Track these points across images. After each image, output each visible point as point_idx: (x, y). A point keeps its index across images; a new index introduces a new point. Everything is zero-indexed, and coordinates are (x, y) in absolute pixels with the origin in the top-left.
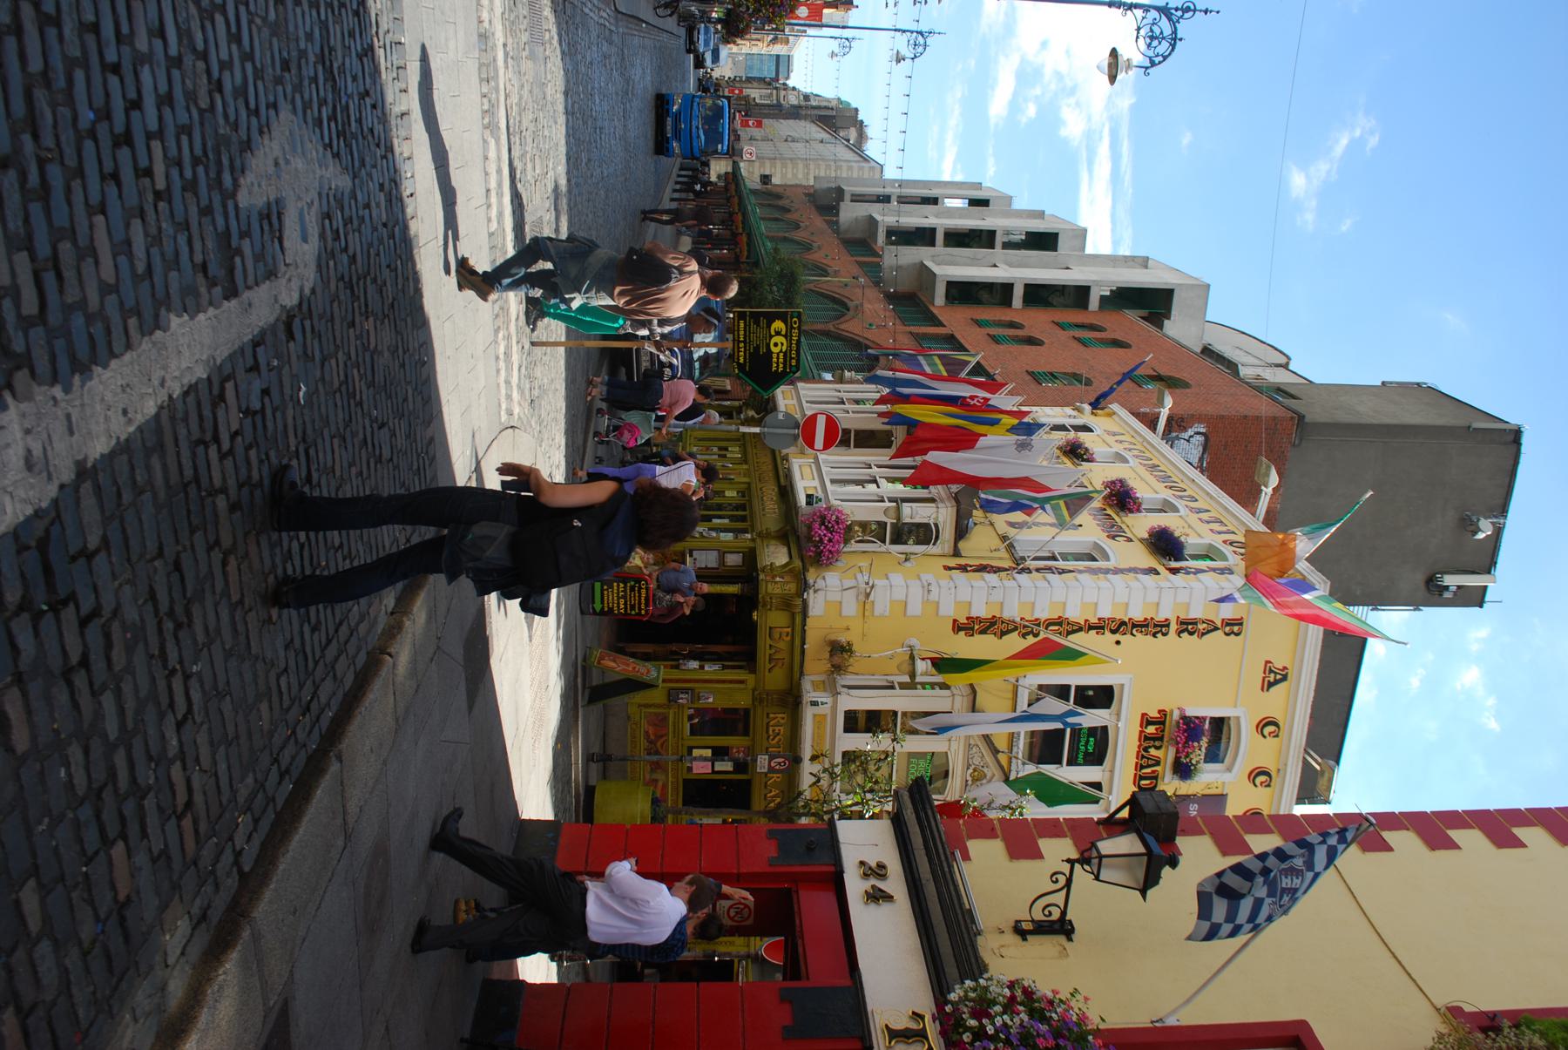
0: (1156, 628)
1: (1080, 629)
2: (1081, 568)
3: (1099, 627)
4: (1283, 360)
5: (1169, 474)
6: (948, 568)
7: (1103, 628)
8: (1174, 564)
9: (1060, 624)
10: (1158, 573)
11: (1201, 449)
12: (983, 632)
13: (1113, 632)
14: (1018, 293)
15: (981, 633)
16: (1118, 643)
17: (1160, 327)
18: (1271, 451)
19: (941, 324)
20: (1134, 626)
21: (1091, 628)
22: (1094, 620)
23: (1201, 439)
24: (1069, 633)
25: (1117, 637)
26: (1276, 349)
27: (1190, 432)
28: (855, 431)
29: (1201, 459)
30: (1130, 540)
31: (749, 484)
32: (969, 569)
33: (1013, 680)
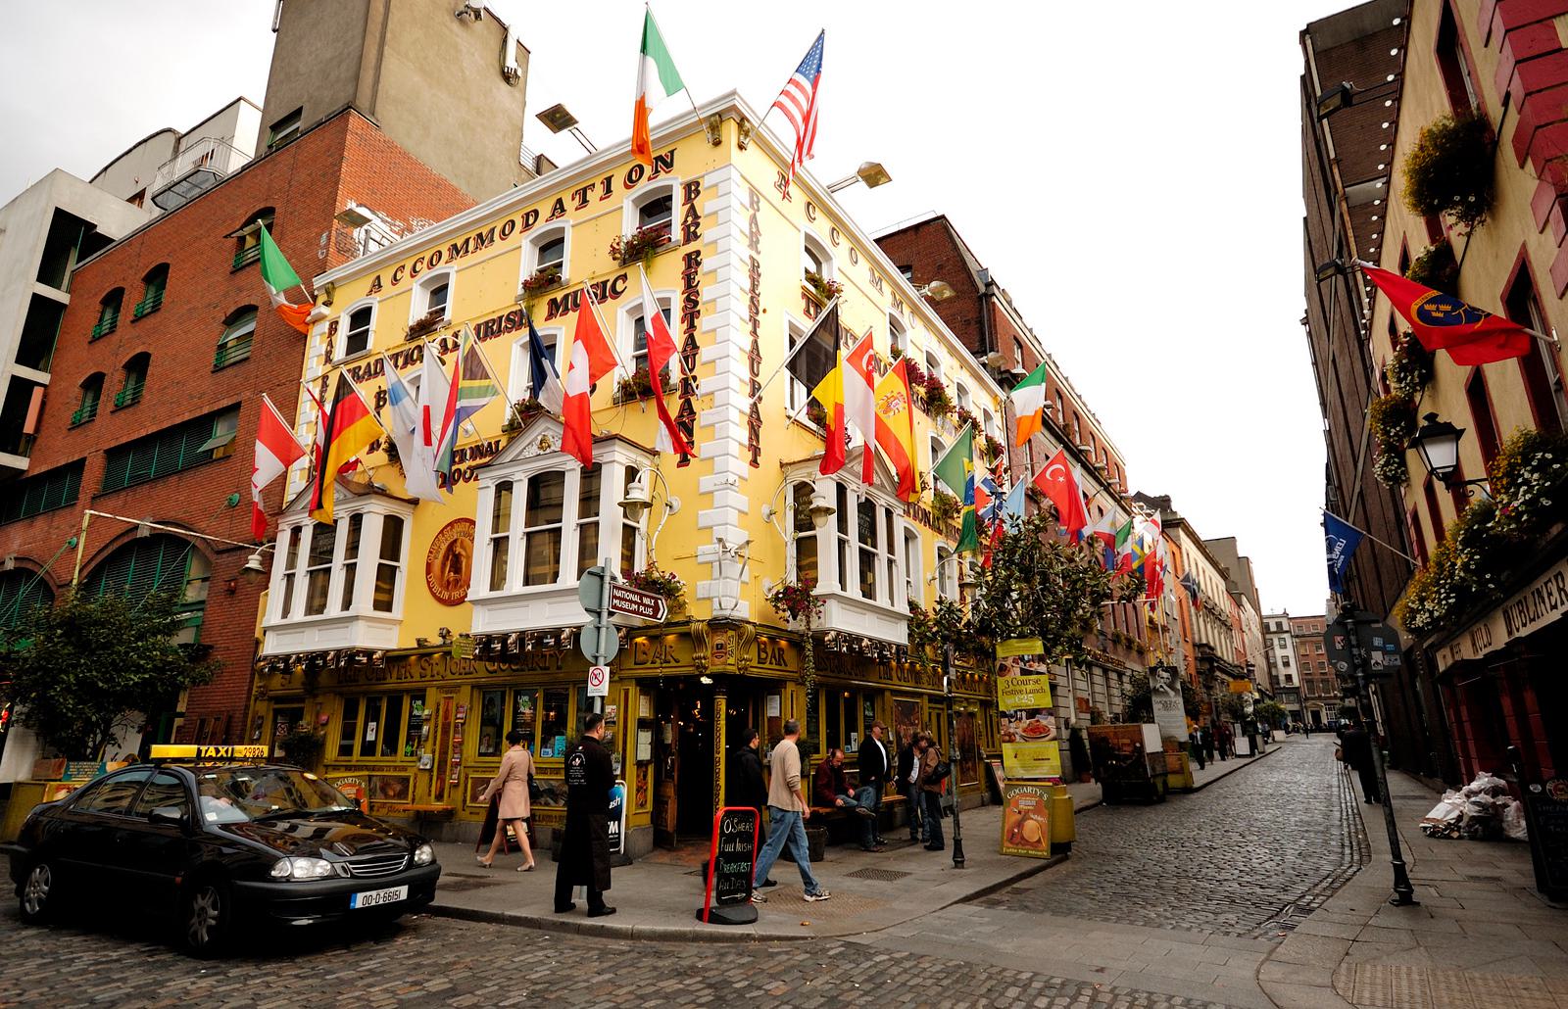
0: (755, 267)
1: (756, 342)
3: (755, 324)
4: (171, 139)
5: (473, 235)
7: (755, 320)
9: (753, 360)
10: (698, 253)
12: (757, 437)
13: (757, 313)
14: (26, 372)
15: (758, 441)
16: (764, 311)
17: (106, 240)
19: (77, 467)
20: (753, 291)
21: (754, 332)
22: (750, 327)
24: (758, 355)
25: (761, 309)
26: (145, 141)
28: (381, 557)
30: (624, 277)
31: (473, 687)
33: (788, 422)
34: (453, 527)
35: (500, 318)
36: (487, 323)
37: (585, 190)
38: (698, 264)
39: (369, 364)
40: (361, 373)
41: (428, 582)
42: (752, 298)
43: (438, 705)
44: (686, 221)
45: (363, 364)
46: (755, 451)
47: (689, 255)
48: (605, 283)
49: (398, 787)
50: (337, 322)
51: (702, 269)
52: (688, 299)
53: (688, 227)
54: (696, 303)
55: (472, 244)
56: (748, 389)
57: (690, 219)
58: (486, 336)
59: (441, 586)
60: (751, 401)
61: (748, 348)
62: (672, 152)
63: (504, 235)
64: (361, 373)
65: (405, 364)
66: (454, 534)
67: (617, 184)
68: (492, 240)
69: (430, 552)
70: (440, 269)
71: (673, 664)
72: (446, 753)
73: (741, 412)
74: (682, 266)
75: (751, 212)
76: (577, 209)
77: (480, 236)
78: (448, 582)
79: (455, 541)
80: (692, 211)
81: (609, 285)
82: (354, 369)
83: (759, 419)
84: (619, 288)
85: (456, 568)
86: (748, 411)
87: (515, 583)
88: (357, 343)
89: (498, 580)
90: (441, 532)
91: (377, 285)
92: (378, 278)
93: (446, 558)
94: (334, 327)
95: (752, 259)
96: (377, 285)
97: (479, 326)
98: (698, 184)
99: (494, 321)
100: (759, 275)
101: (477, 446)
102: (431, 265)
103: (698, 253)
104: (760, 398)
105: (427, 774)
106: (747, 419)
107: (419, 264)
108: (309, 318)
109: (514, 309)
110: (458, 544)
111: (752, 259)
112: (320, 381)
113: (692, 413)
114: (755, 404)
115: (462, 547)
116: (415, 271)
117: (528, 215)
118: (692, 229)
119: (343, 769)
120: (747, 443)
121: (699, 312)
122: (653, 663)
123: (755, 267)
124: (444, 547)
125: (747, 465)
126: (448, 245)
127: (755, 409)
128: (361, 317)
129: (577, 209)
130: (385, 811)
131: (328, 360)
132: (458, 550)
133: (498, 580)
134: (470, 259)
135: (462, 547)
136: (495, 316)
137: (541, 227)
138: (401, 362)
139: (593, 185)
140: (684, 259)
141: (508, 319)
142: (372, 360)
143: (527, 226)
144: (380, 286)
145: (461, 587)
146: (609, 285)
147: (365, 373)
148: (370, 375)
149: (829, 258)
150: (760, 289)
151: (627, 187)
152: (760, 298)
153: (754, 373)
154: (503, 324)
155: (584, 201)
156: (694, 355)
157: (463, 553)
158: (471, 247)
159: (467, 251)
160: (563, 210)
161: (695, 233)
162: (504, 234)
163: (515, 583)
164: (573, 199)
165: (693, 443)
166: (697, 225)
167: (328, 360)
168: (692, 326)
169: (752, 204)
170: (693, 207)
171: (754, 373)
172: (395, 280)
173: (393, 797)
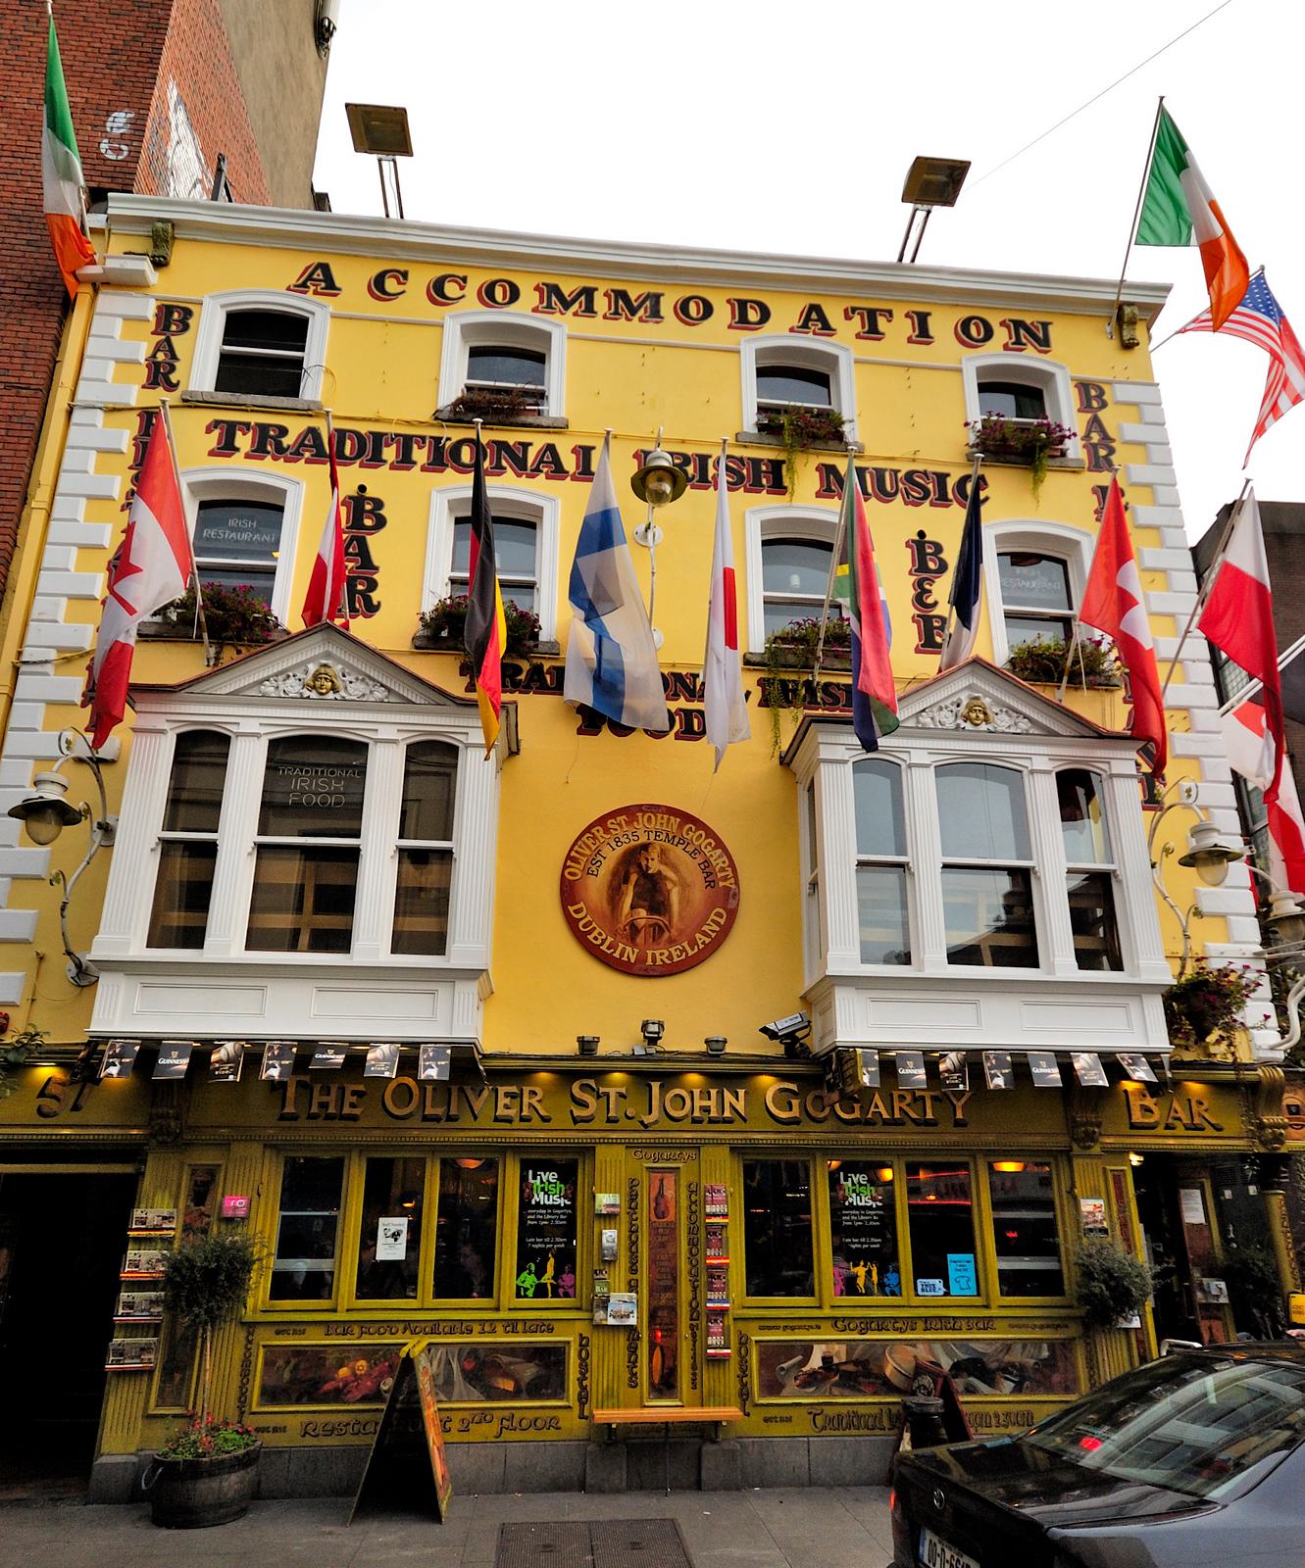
40: (287, 441)
41: (572, 923)
43: (633, 1184)
45: (296, 427)
49: (529, 1371)
50: (188, 313)
57: (1095, 438)
59: (614, 935)
62: (1045, 325)
67: (943, 324)
69: (569, 857)
71: (1209, 1131)
72: (672, 1288)
78: (634, 930)
79: (645, 847)
80: (1096, 423)
82: (263, 428)
90: (602, 821)
93: (619, 877)
94: (173, 318)
101: (678, 677)
105: (622, 1341)
110: (654, 853)
112: (134, 422)
118: (1103, 452)
119: (322, 1330)
122: (1167, 1127)
124: (611, 856)
130: (494, 1427)
132: (654, 866)
134: (596, 326)
137: (781, 332)
138: (420, 455)
145: (671, 942)
146: (951, 483)
157: (670, 874)
166: (1112, 451)
173: (516, 1394)
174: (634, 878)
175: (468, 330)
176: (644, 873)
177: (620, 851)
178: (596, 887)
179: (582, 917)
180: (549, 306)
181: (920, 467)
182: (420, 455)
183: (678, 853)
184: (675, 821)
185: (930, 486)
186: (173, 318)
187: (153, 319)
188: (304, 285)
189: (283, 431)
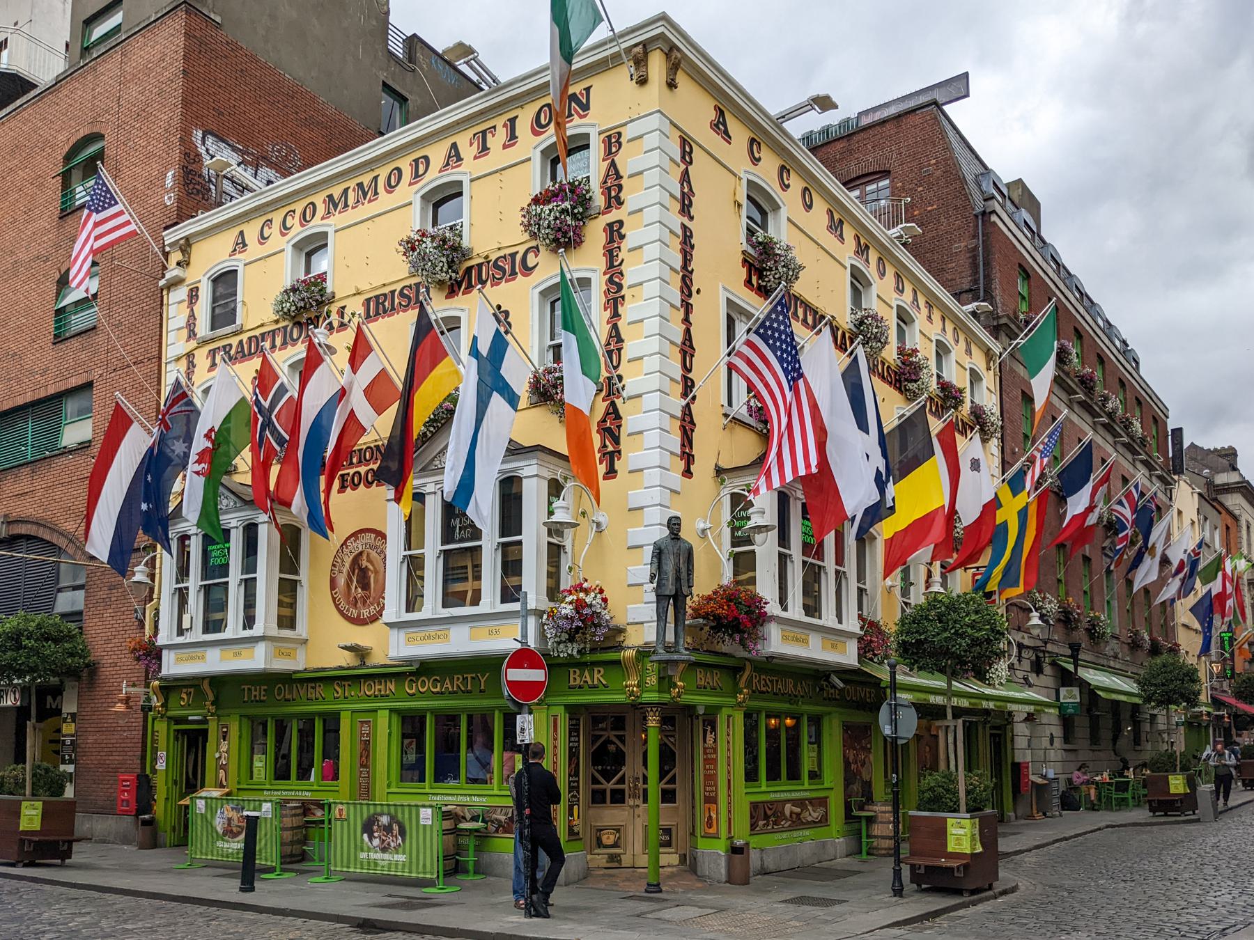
2: (608, 314)
5: (352, 184)
6: (611, 473)
8: (599, 200)
10: (621, 223)
11: (222, 145)
18: (226, 57)
23: (210, 140)
27: (202, 150)
29: (234, 149)
32: (610, 448)
34: (357, 538)
35: (393, 292)
36: (377, 297)
37: (484, 133)
38: (622, 237)
39: (241, 342)
40: (232, 352)
42: (684, 278)
44: (605, 182)
45: (234, 341)
46: (688, 458)
47: (610, 225)
48: (513, 255)
50: (197, 288)
51: (625, 245)
52: (611, 281)
53: (609, 189)
54: (620, 287)
55: (351, 195)
56: (679, 389)
58: (377, 314)
60: (684, 402)
61: (679, 340)
63: (390, 187)
64: (232, 352)
65: (284, 344)
66: (357, 546)
68: (376, 193)
70: (316, 225)
73: (672, 416)
74: (602, 238)
75: (683, 167)
76: (475, 158)
77: (360, 185)
79: (361, 553)
81: (518, 257)
82: (224, 347)
83: (692, 422)
84: (530, 264)
85: (365, 585)
86: (679, 414)
87: (431, 605)
88: (223, 314)
89: (413, 600)
90: (345, 543)
91: (241, 244)
92: (241, 233)
94: (193, 295)
95: (684, 227)
96: (241, 244)
97: (368, 300)
98: (620, 134)
99: (385, 295)
100: (692, 247)
102: (304, 220)
103: (621, 223)
104: (694, 398)
106: (678, 423)
107: (289, 218)
108: (162, 283)
109: (407, 283)
111: (684, 227)
112: (184, 362)
113: (618, 417)
114: (688, 405)
115: (369, 560)
116: (286, 228)
117: (416, 161)
120: (678, 451)
121: (623, 297)
123: (687, 235)
124: (348, 561)
125: (680, 476)
126: (324, 194)
127: (687, 410)
128: (225, 281)
129: (475, 158)
131: (192, 334)
132: (365, 563)
133: (413, 600)
135: (369, 560)
136: (386, 290)
138: (278, 341)
139: (494, 127)
140: (605, 230)
141: (402, 294)
142: (244, 337)
143: (417, 176)
144: (245, 245)
146: (518, 257)
147: (237, 352)
148: (244, 356)
149: (776, 208)
150: (693, 265)
151: (536, 133)
152: (694, 277)
153: (687, 369)
154: (397, 301)
155: (484, 149)
156: (620, 350)
157: (370, 567)
158: (351, 201)
159: (346, 205)
160: (459, 159)
161: (617, 198)
162: (389, 185)
163: (431, 605)
164: (471, 144)
165: (619, 452)
167: (192, 334)
168: (616, 315)
169: (683, 158)
170: (613, 164)
171: (687, 369)
172: (263, 238)
174: (357, 571)
175: (298, 247)
176: (361, 569)
177: (351, 557)
178: (342, 581)
179: (339, 596)
180: (329, 213)
181: (501, 253)
182: (278, 341)
183: (373, 554)
184: (373, 536)
185: (507, 267)
186: (193, 295)
187: (186, 298)
188: (235, 250)
189: (230, 345)
